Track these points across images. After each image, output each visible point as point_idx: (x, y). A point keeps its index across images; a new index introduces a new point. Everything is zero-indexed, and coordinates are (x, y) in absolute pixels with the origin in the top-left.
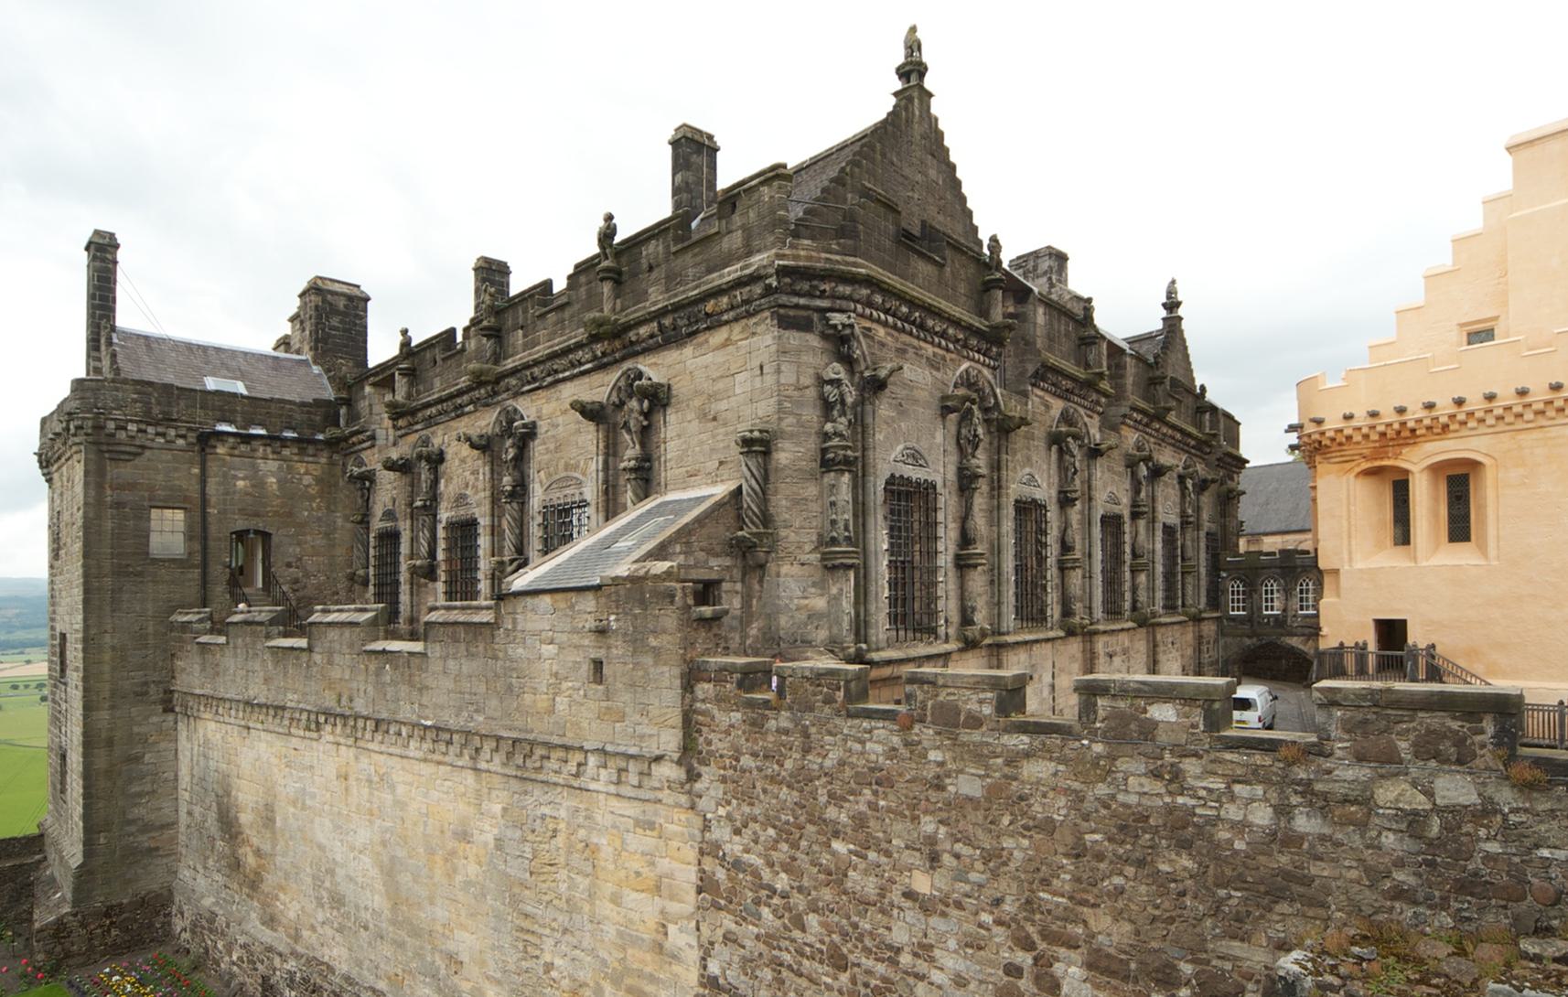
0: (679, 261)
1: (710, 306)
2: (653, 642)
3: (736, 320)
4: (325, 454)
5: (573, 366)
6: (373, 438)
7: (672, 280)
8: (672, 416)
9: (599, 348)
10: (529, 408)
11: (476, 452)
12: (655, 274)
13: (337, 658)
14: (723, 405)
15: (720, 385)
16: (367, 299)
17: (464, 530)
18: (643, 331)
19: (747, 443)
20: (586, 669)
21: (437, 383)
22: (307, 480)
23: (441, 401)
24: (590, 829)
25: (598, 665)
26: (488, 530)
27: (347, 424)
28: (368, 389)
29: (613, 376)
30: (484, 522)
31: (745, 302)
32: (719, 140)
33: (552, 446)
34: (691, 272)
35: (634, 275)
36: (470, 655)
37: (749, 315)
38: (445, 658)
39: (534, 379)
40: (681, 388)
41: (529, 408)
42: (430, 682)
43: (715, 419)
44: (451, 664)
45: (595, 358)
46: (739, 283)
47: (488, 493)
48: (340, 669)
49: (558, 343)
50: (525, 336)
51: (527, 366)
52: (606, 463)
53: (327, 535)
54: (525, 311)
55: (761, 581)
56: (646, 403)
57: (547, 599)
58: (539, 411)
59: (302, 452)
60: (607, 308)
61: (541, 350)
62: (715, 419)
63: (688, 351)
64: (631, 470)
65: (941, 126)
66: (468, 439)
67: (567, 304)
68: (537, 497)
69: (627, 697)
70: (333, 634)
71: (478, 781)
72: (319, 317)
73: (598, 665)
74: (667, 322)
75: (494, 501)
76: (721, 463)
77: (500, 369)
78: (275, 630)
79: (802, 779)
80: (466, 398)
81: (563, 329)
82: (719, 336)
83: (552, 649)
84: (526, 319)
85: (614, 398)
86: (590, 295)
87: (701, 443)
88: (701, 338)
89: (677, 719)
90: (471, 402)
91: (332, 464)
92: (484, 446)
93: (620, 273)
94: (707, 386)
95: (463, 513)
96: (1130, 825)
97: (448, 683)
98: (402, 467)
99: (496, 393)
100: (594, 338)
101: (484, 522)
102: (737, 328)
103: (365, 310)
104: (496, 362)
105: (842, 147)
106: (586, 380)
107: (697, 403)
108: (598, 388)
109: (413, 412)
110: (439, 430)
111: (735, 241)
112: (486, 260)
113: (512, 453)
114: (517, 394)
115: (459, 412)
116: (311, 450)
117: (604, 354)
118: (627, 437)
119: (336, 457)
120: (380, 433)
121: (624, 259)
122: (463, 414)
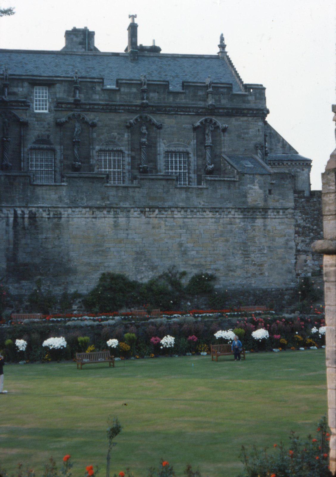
1: (245, 112)
3: (250, 116)
8: (226, 134)
14: (246, 136)
18: (221, 111)
29: (203, 119)
37: (256, 116)
43: (243, 138)
45: (196, 112)
62: (243, 138)
76: (245, 150)
80: (121, 108)
88: (238, 118)
102: (250, 119)
106: (188, 117)
107: (237, 133)
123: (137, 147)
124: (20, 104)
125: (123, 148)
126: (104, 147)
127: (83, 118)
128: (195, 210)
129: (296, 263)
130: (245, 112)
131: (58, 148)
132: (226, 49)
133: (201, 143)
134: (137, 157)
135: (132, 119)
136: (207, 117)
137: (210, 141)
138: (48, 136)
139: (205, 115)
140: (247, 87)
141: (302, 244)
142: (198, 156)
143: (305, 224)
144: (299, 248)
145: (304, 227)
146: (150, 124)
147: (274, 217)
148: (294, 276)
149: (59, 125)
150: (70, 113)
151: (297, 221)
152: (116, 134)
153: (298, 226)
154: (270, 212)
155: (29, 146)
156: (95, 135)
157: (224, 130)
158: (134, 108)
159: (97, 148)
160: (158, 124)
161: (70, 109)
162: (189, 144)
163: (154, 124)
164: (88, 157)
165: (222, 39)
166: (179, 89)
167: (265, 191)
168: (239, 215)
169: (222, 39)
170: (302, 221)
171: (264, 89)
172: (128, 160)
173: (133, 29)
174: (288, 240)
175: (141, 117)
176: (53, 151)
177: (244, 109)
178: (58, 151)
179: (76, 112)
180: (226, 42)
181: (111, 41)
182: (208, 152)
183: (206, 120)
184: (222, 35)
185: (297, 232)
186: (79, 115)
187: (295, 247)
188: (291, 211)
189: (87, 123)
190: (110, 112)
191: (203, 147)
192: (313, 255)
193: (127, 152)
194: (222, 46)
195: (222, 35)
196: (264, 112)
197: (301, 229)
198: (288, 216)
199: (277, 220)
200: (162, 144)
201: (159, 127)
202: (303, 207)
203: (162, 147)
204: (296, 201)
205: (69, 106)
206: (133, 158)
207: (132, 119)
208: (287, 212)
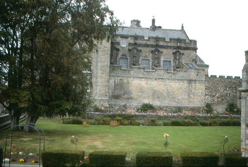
8: (183, 55)
14: (190, 56)
18: (182, 48)
25: (197, 75)
28: (119, 37)
29: (176, 50)
41: (161, 50)
63: (186, 51)
79: (213, 81)
82: (190, 51)
96: (230, 82)
102: (191, 51)
106: (171, 49)
107: (187, 55)
123: (154, 58)
125: (150, 59)
126: (143, 58)
127: (137, 49)
129: (205, 98)
130: (190, 48)
131: (129, 58)
132: (184, 28)
133: (175, 58)
134: (154, 62)
135: (153, 49)
137: (178, 57)
138: (126, 54)
139: (177, 49)
140: (191, 41)
142: (174, 62)
143: (208, 86)
144: (206, 93)
145: (208, 87)
146: (159, 51)
148: (204, 103)
149: (129, 50)
150: (133, 47)
152: (147, 54)
153: (206, 86)
154: (197, 81)
155: (120, 57)
156: (141, 54)
157: (183, 54)
159: (141, 58)
160: (161, 51)
161: (133, 46)
162: (171, 58)
163: (160, 51)
164: (138, 61)
165: (183, 25)
166: (169, 40)
167: (196, 75)
169: (183, 25)
171: (197, 41)
172: (151, 63)
173: (153, 21)
174: (202, 91)
175: (156, 49)
176: (127, 59)
177: (189, 48)
178: (129, 59)
179: (135, 46)
180: (183, 26)
181: (146, 24)
182: (177, 61)
183: (177, 51)
185: (205, 88)
186: (136, 48)
187: (204, 93)
188: (204, 81)
189: (138, 50)
191: (176, 60)
192: (211, 96)
193: (151, 60)
194: (183, 27)
196: (195, 49)
197: (207, 88)
199: (199, 84)
200: (162, 58)
201: (162, 53)
202: (208, 80)
203: (162, 59)
204: (206, 78)
205: (133, 44)
206: (153, 62)
207: (153, 49)
208: (203, 82)
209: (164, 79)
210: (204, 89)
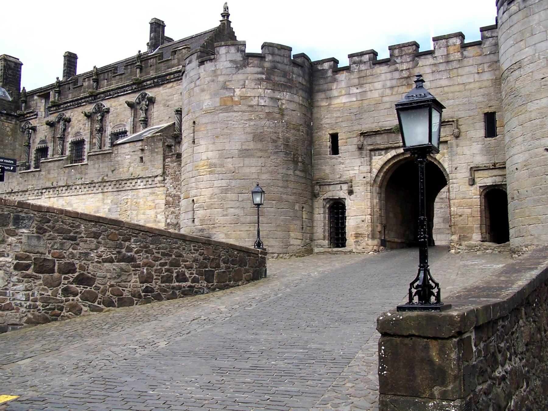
0: (160, 65)
2: (156, 150)
4: (14, 120)
5: (124, 91)
6: (37, 115)
7: (157, 70)
8: (155, 106)
9: (134, 87)
10: (106, 104)
11: (86, 117)
12: (152, 68)
13: (52, 172)
14: (171, 103)
15: (170, 98)
16: (22, 64)
17: (78, 145)
18: (148, 82)
19: (177, 111)
20: (139, 159)
21: (70, 96)
22: (8, 129)
23: (70, 102)
24: (137, 199)
25: (142, 158)
26: (89, 143)
27: (25, 110)
28: (36, 97)
29: (137, 95)
30: (87, 140)
31: (177, 77)
32: (166, 23)
33: (115, 115)
34: (163, 68)
35: (146, 67)
36: (103, 162)
38: (94, 164)
39: (110, 95)
40: (158, 99)
41: (106, 104)
42: (89, 171)
44: (97, 166)
46: (176, 72)
47: (89, 131)
48: (54, 174)
49: (120, 85)
50: (107, 82)
51: (109, 91)
52: (134, 119)
53: (13, 150)
54: (108, 75)
55: (179, 147)
56: (147, 102)
57: (128, 145)
58: (111, 105)
59: (7, 119)
60: (138, 76)
61: (113, 87)
63: (161, 88)
64: (142, 121)
65: (234, 30)
66: (85, 113)
67: (124, 74)
68: (109, 130)
69: (149, 164)
70: (50, 165)
71: (103, 195)
72: (5, 70)
73: (142, 158)
74: (156, 80)
75: (91, 133)
77: (98, 92)
78: (22, 168)
80: (83, 100)
81: (122, 81)
83: (129, 156)
84: (108, 77)
85: (137, 101)
86: (131, 72)
87: (164, 112)
89: (162, 166)
90: (85, 102)
91: (16, 124)
92: (89, 116)
93: (142, 66)
94: (166, 98)
95: (78, 138)
97: (95, 171)
98: (51, 125)
99: (95, 99)
100: (134, 84)
101: (87, 140)
102: (175, 83)
103: (21, 69)
104: (97, 90)
105: (205, 33)
106: (128, 96)
107: (163, 102)
108: (133, 98)
109: (59, 105)
110: (69, 111)
111: (175, 61)
112: (69, 53)
113: (100, 118)
114: (102, 100)
115: (79, 105)
116: (10, 118)
117: (135, 88)
118: (141, 112)
119: (18, 122)
120: (39, 113)
121: (143, 63)
122: (81, 106)
124: (32, 114)
128: (78, 187)
136: (141, 92)
141: (171, 216)
144: (168, 221)
145: (175, 196)
147: (144, 187)
151: (168, 190)
156: (70, 128)
158: (90, 98)
159: (70, 139)
165: (226, 8)
168: (113, 188)
169: (226, 8)
170: (172, 189)
174: (157, 213)
184: (226, 3)
185: (167, 203)
190: (78, 107)
193: (86, 140)
194: (226, 15)
195: (226, 3)
197: (171, 199)
198: (158, 185)
207: (90, 108)
209: (60, 187)
210: (163, 207)
